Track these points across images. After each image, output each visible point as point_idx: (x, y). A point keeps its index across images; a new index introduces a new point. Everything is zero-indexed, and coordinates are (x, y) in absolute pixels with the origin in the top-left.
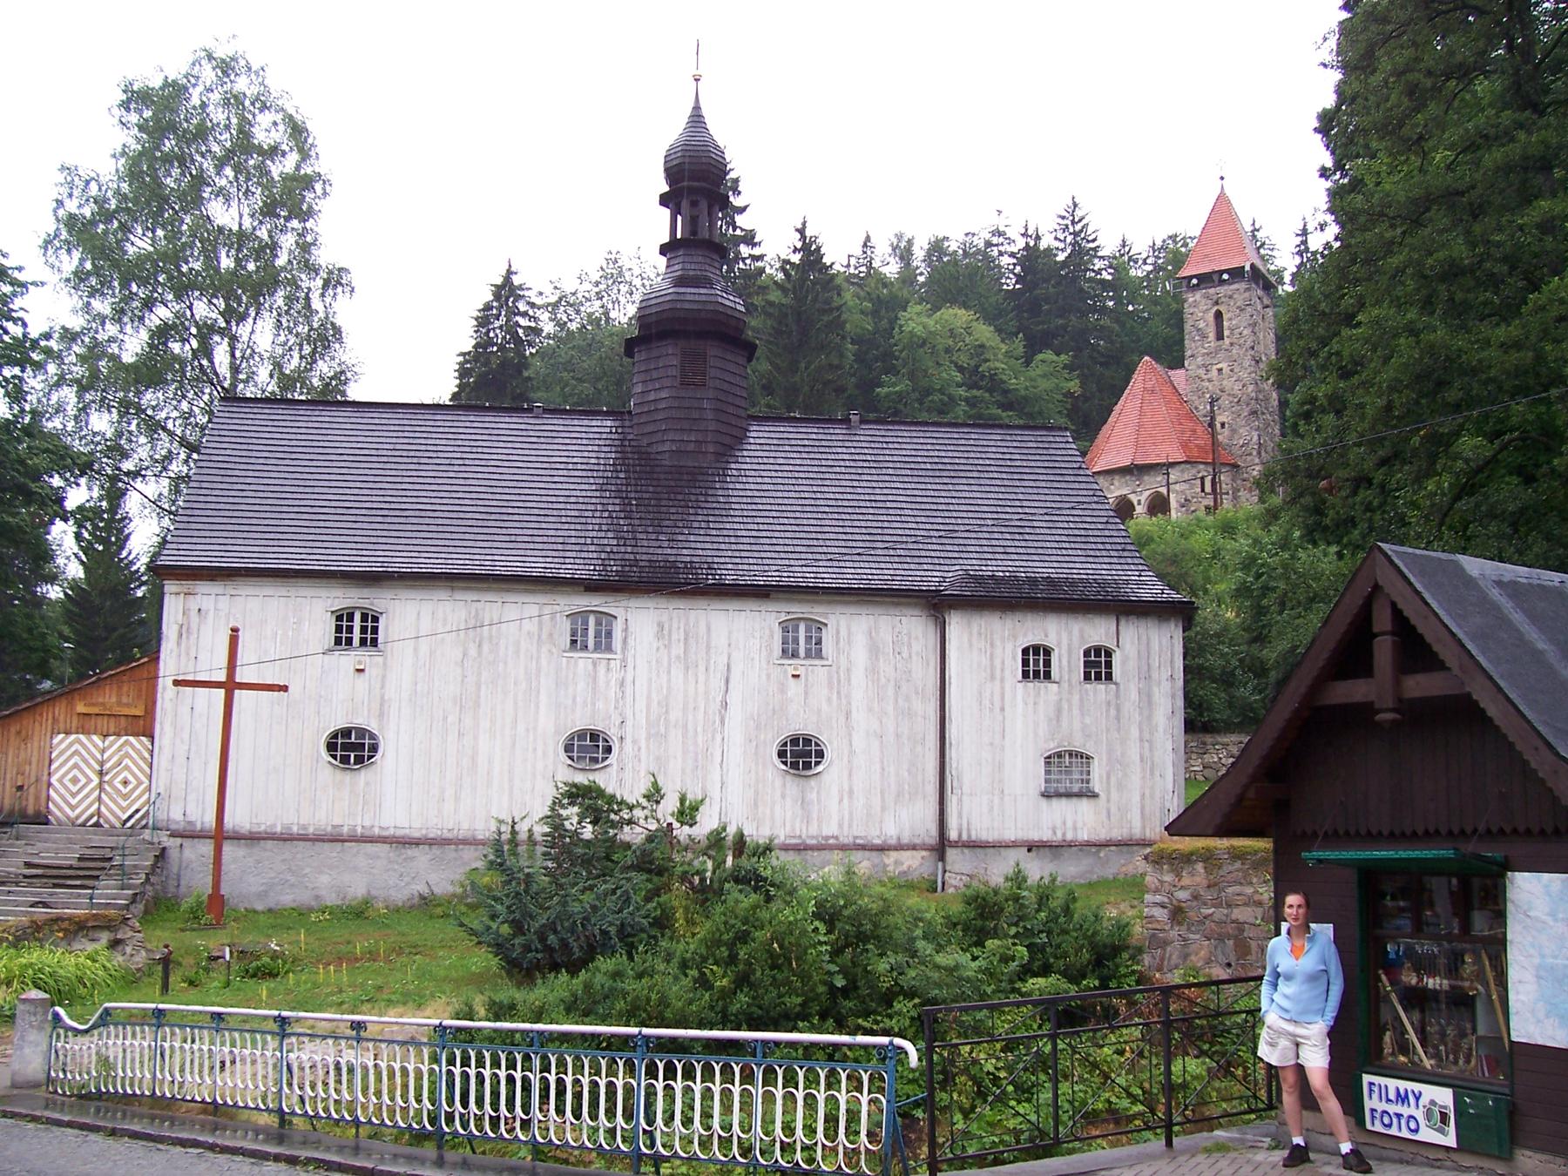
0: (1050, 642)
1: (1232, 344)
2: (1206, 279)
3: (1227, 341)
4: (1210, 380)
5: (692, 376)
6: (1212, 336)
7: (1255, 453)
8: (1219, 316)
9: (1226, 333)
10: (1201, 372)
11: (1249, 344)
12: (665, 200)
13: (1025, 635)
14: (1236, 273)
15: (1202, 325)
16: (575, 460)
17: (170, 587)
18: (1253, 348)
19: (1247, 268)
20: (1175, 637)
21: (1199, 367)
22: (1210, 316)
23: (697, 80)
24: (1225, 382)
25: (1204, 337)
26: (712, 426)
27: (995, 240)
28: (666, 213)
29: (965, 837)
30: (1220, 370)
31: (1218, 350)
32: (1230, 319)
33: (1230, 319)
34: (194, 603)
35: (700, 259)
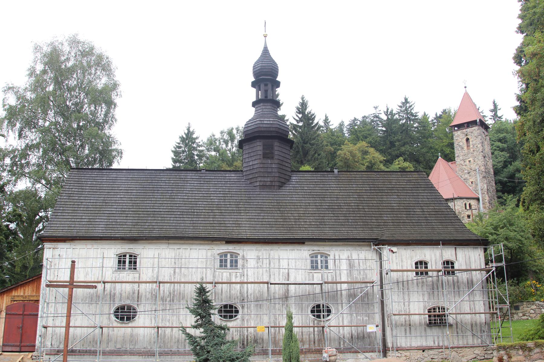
0: (427, 258)
1: (474, 151)
2: (460, 126)
3: (472, 150)
4: (466, 165)
5: (267, 155)
6: (465, 148)
7: (486, 193)
8: (468, 140)
9: (471, 146)
10: (462, 162)
11: (481, 150)
12: (254, 85)
13: (416, 256)
14: (473, 123)
15: (461, 144)
16: (220, 190)
17: (47, 245)
18: (482, 152)
19: (478, 121)
20: (481, 255)
21: (461, 160)
22: (464, 140)
23: (265, 37)
24: (472, 166)
25: (462, 148)
26: (277, 175)
27: (375, 119)
28: (254, 90)
29: (395, 346)
30: (470, 161)
31: (468, 153)
32: (473, 141)
33: (473, 141)
34: (57, 252)
35: (269, 107)
